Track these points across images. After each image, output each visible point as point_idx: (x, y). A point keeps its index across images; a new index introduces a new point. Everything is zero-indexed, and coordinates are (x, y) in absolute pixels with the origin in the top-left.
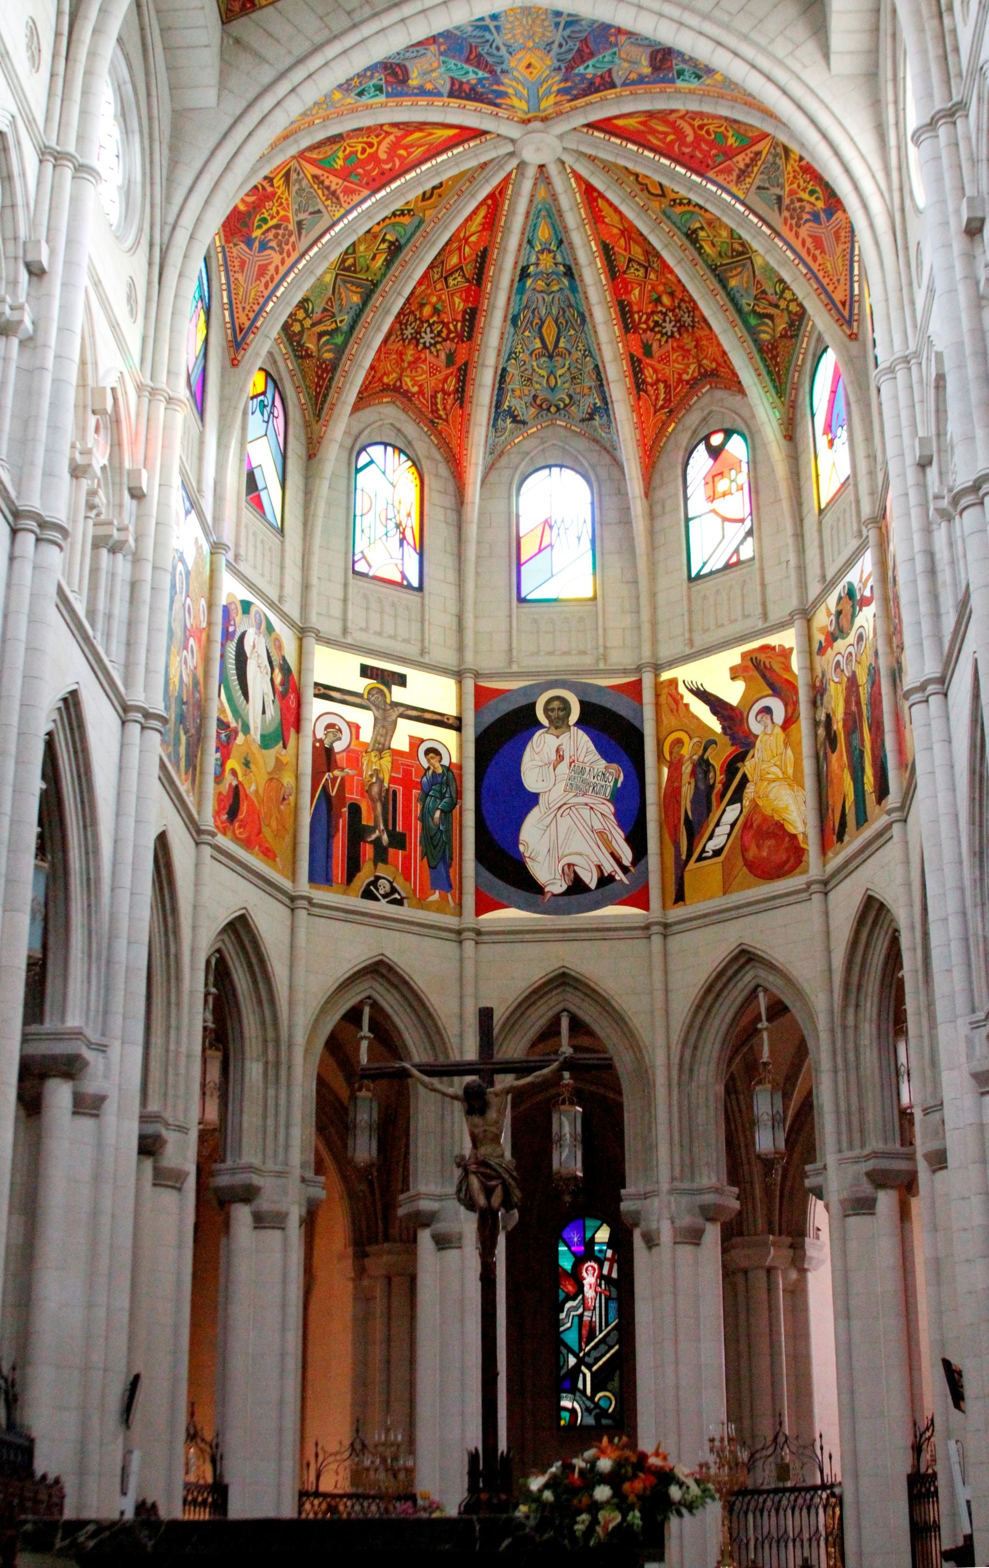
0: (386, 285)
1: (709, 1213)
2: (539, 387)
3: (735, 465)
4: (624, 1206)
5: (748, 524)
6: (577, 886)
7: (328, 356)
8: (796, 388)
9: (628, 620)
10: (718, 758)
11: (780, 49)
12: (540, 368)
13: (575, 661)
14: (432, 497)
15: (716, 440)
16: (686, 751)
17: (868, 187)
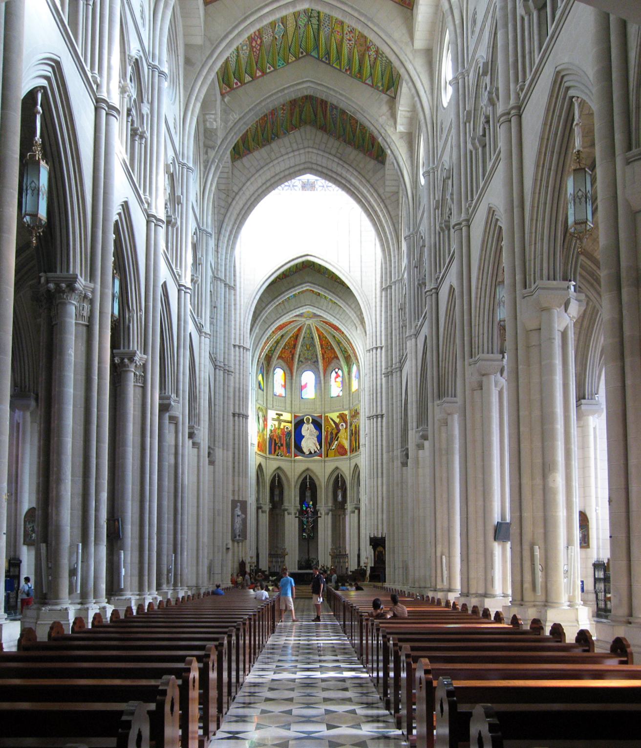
0: (281, 342)
1: (331, 510)
2: (306, 356)
3: (339, 376)
4: (317, 508)
5: (341, 389)
6: (311, 453)
7: (270, 355)
8: (350, 365)
9: (320, 403)
10: (335, 432)
11: (349, 327)
12: (306, 352)
13: (311, 410)
14: (287, 380)
15: (337, 370)
16: (329, 430)
17: (361, 356)
